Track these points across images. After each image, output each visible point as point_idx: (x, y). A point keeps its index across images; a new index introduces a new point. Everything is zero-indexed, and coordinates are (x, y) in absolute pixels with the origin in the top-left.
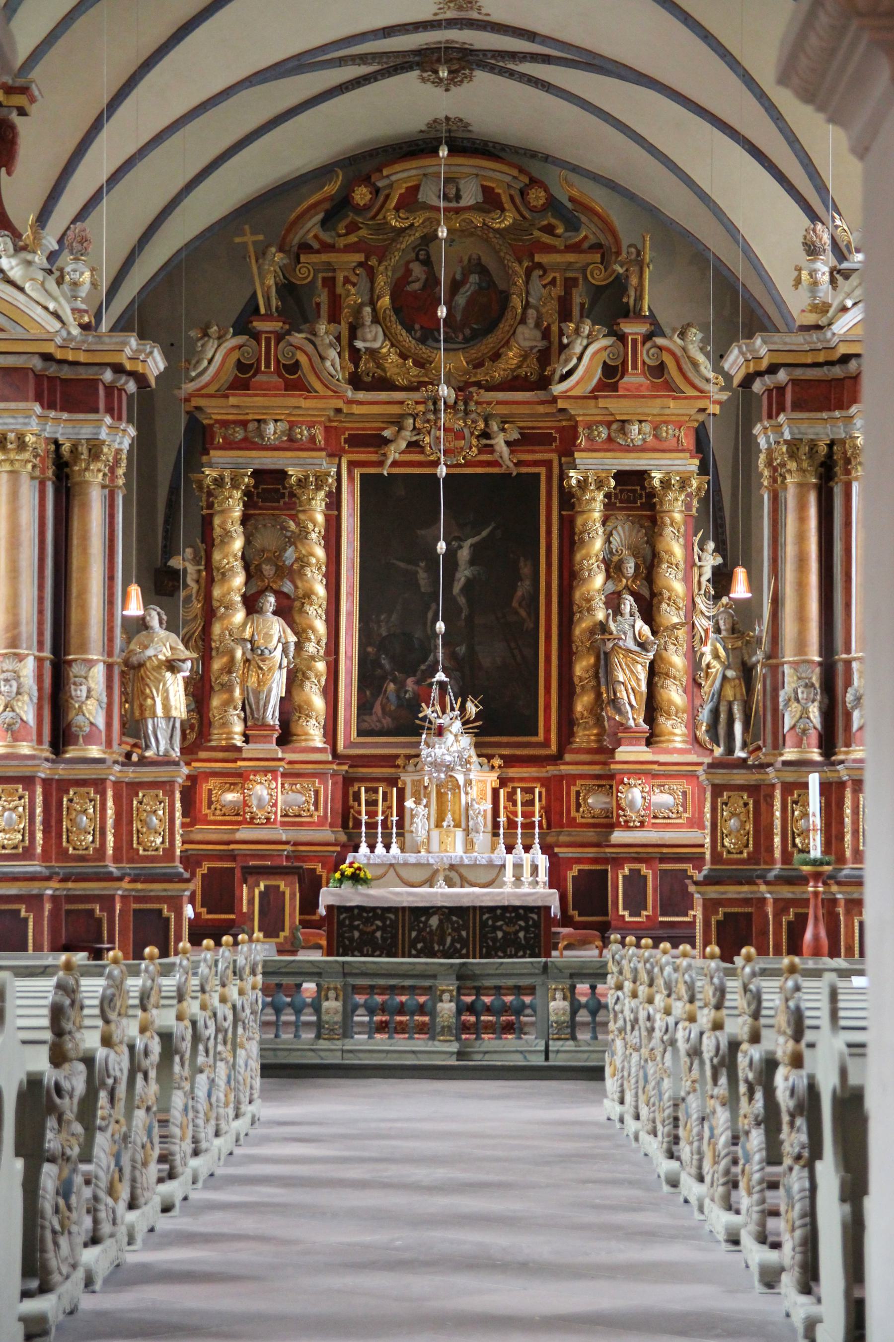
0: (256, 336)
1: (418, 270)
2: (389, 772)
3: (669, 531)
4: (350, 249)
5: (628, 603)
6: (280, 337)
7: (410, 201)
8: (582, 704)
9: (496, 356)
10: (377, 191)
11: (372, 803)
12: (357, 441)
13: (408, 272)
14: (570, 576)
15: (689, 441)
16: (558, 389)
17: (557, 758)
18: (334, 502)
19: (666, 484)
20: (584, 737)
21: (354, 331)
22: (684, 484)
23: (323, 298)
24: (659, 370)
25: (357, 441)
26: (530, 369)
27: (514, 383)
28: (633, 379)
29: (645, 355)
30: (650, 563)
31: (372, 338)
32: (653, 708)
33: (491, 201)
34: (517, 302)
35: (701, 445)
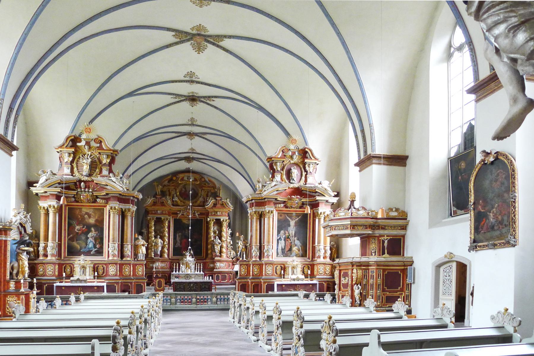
0: (157, 198)
1: (183, 189)
2: (178, 262)
3: (224, 227)
4: (173, 186)
5: (217, 237)
6: (161, 198)
7: (182, 179)
8: (209, 252)
9: (196, 202)
10: (177, 178)
11: (176, 265)
12: (173, 213)
13: (182, 189)
14: (208, 233)
15: (227, 215)
16: (206, 207)
17: (205, 259)
18: (169, 222)
19: (223, 221)
20: (210, 256)
21: (173, 198)
22: (226, 220)
23: (168, 193)
24: (223, 204)
25: (173, 213)
26: (202, 204)
27: (199, 206)
28: (218, 206)
29: (220, 202)
30: (220, 231)
31: (176, 199)
32: (221, 252)
33: (195, 180)
34: (200, 195)
35: (229, 216)
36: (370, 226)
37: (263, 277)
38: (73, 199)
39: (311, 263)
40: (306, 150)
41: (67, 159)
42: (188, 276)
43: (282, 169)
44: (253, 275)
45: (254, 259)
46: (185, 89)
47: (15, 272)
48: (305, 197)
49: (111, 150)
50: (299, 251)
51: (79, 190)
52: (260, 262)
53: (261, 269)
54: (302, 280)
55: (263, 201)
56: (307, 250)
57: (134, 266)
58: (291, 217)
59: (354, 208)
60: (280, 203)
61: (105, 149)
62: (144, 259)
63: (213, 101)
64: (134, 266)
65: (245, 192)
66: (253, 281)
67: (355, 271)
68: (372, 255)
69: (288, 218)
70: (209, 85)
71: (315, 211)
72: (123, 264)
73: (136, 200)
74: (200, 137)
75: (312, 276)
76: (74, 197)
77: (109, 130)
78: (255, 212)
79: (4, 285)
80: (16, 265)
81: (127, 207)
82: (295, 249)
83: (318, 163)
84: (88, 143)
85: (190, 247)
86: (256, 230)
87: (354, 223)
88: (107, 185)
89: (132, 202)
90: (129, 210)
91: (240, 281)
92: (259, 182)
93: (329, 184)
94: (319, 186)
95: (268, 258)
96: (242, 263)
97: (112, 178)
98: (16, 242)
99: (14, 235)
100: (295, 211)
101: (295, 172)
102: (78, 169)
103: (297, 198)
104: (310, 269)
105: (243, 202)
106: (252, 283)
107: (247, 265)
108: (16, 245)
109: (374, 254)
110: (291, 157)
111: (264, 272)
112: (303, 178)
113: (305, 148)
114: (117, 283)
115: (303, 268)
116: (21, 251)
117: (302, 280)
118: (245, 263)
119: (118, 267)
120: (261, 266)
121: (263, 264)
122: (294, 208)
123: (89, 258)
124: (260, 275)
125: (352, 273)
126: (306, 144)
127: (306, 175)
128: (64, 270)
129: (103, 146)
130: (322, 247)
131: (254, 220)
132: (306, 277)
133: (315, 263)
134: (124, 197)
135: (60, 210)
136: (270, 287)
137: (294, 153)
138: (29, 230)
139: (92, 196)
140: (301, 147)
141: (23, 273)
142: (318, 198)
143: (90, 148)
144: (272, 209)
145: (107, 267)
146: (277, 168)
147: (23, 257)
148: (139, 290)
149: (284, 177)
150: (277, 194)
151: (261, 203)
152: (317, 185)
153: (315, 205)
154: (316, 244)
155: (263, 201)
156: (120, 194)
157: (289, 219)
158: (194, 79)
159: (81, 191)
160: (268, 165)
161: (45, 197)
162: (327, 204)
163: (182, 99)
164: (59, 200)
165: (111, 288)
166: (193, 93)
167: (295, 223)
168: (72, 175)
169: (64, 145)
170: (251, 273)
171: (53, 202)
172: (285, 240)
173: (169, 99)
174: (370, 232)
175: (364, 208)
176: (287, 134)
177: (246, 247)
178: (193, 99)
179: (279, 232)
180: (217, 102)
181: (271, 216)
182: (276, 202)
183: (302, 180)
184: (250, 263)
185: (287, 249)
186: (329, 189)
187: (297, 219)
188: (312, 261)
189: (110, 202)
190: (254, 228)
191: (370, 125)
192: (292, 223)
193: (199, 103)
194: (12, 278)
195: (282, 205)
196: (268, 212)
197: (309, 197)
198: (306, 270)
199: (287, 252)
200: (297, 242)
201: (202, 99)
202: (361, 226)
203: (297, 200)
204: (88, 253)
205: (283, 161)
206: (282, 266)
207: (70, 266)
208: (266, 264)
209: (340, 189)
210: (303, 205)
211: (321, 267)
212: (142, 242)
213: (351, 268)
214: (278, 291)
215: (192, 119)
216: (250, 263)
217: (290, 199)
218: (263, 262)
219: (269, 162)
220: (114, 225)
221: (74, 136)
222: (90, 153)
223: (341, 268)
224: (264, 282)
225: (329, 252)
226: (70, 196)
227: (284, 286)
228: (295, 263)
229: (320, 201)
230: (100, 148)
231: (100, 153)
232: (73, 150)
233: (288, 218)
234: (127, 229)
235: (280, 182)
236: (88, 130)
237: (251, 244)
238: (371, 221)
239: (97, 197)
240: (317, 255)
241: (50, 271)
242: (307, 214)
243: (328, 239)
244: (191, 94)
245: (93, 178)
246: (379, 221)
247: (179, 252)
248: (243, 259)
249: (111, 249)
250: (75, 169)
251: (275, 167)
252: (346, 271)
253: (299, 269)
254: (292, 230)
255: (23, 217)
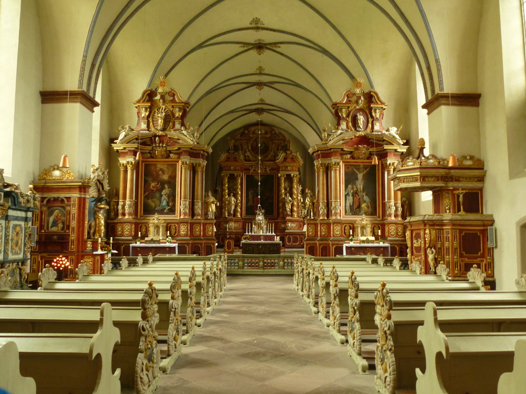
36: (442, 177)
37: (331, 239)
38: (149, 155)
39: (382, 222)
40: (372, 93)
41: (144, 114)
42: (258, 238)
43: (348, 116)
44: (321, 236)
45: (321, 218)
46: (252, 37)
47: (92, 231)
48: (372, 147)
49: (183, 103)
50: (368, 208)
51: (154, 145)
52: (328, 221)
53: (329, 229)
54: (372, 242)
55: (329, 151)
56: (377, 208)
57: (205, 225)
58: (358, 170)
59: (424, 156)
60: (347, 154)
61: (178, 101)
62: (214, 218)
63: (279, 47)
64: (205, 225)
65: (313, 141)
66: (321, 242)
67: (427, 231)
68: (446, 212)
69: (355, 170)
70: (274, 30)
71: (383, 162)
72: (193, 224)
73: (206, 154)
74: (269, 86)
75: (383, 237)
76: (149, 153)
77: (183, 84)
78: (321, 164)
79: (82, 245)
80: (93, 224)
81: (198, 162)
82: (363, 205)
83: (384, 107)
84: (163, 97)
85: (259, 205)
86: (323, 184)
87: (424, 174)
88: (179, 139)
89: (203, 157)
90: (199, 165)
91: (308, 242)
92: (324, 131)
93: (397, 131)
94: (387, 133)
95: (336, 216)
96: (309, 222)
97: (184, 132)
98: (93, 199)
99: (92, 193)
100: (362, 162)
101: (361, 119)
102: (153, 124)
103: (364, 147)
104: (380, 228)
105: (309, 153)
106: (320, 245)
107: (315, 224)
108: (94, 203)
109: (448, 211)
110: (357, 102)
111: (332, 233)
112: (370, 125)
113: (371, 92)
114: (188, 244)
115: (374, 229)
116: (98, 209)
117: (372, 242)
118: (312, 222)
119: (189, 226)
120: (329, 225)
121: (330, 223)
122: (361, 159)
123: (163, 217)
124: (328, 236)
125: (425, 234)
126: (372, 87)
127: (373, 122)
128: (140, 229)
129: (176, 99)
130: (392, 203)
131: (321, 173)
132: (377, 239)
133: (386, 222)
134: (195, 151)
135: (136, 166)
136: (339, 250)
137: (359, 98)
138: (107, 188)
139: (166, 151)
140: (366, 91)
141: (100, 230)
142: (386, 147)
143: (164, 102)
144: (338, 161)
145: (179, 227)
146: (342, 115)
147: (100, 215)
148: (209, 251)
149: (350, 124)
150: (343, 144)
151: (327, 153)
152: (384, 132)
153: (383, 155)
154: (386, 200)
155: (329, 151)
156: (191, 148)
157: (357, 171)
158: (259, 25)
159: (156, 146)
160: (333, 111)
161: (124, 154)
162: (396, 153)
163: (250, 47)
164: (136, 156)
165: (182, 250)
166: (259, 40)
167: (363, 176)
168: (148, 130)
169: (140, 100)
170: (319, 233)
171: (131, 159)
172: (353, 195)
173: (237, 48)
174: (443, 185)
175: (434, 156)
176: (352, 77)
177: (313, 204)
178: (260, 47)
179: (346, 187)
180: (283, 49)
181: (338, 169)
182: (342, 153)
183: (368, 128)
184: (318, 222)
185: (355, 207)
186: (397, 136)
187: (365, 172)
188: (383, 220)
189: (182, 157)
190: (321, 182)
191: (437, 61)
192: (360, 176)
193: (266, 50)
194: (89, 237)
195: (349, 156)
196: (335, 164)
197: (377, 145)
198: (376, 231)
199: (355, 209)
200: (366, 198)
201: (269, 46)
202: (432, 177)
203: (363, 149)
204: (161, 212)
205: (349, 107)
206: (351, 225)
207: (145, 225)
208: (334, 223)
209: (409, 136)
210: (370, 157)
211: (393, 228)
212: (212, 199)
213: (423, 227)
214: (347, 254)
215: (260, 68)
216: (318, 222)
217: (357, 149)
218: (331, 221)
219: (334, 108)
220: (185, 181)
221: (150, 90)
222: (164, 107)
223: (413, 228)
224: (333, 245)
225: (400, 209)
226: (146, 151)
227: (353, 249)
228: (364, 222)
229: (388, 151)
230: (173, 101)
231: (173, 106)
232: (149, 104)
233: (355, 170)
234: (198, 185)
235: (346, 131)
236: (163, 84)
237: (318, 200)
238: (442, 172)
239: (170, 152)
240: (388, 213)
241: (127, 231)
242: (375, 166)
243: (399, 193)
244: (257, 42)
245: (167, 132)
246: (452, 171)
247: (251, 211)
248: (310, 217)
249: (182, 206)
250: (151, 124)
251: (340, 114)
252: (418, 232)
253: (369, 230)
254: (360, 184)
255: (100, 174)
